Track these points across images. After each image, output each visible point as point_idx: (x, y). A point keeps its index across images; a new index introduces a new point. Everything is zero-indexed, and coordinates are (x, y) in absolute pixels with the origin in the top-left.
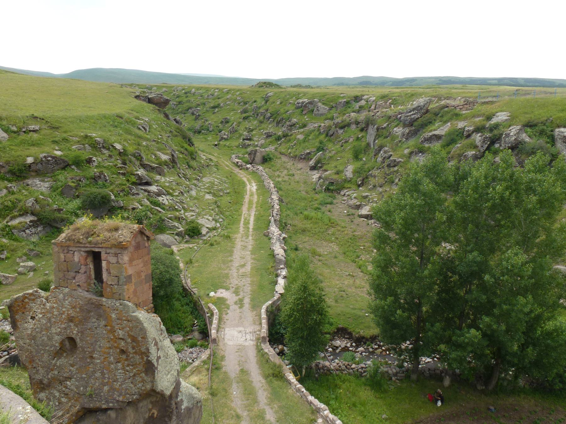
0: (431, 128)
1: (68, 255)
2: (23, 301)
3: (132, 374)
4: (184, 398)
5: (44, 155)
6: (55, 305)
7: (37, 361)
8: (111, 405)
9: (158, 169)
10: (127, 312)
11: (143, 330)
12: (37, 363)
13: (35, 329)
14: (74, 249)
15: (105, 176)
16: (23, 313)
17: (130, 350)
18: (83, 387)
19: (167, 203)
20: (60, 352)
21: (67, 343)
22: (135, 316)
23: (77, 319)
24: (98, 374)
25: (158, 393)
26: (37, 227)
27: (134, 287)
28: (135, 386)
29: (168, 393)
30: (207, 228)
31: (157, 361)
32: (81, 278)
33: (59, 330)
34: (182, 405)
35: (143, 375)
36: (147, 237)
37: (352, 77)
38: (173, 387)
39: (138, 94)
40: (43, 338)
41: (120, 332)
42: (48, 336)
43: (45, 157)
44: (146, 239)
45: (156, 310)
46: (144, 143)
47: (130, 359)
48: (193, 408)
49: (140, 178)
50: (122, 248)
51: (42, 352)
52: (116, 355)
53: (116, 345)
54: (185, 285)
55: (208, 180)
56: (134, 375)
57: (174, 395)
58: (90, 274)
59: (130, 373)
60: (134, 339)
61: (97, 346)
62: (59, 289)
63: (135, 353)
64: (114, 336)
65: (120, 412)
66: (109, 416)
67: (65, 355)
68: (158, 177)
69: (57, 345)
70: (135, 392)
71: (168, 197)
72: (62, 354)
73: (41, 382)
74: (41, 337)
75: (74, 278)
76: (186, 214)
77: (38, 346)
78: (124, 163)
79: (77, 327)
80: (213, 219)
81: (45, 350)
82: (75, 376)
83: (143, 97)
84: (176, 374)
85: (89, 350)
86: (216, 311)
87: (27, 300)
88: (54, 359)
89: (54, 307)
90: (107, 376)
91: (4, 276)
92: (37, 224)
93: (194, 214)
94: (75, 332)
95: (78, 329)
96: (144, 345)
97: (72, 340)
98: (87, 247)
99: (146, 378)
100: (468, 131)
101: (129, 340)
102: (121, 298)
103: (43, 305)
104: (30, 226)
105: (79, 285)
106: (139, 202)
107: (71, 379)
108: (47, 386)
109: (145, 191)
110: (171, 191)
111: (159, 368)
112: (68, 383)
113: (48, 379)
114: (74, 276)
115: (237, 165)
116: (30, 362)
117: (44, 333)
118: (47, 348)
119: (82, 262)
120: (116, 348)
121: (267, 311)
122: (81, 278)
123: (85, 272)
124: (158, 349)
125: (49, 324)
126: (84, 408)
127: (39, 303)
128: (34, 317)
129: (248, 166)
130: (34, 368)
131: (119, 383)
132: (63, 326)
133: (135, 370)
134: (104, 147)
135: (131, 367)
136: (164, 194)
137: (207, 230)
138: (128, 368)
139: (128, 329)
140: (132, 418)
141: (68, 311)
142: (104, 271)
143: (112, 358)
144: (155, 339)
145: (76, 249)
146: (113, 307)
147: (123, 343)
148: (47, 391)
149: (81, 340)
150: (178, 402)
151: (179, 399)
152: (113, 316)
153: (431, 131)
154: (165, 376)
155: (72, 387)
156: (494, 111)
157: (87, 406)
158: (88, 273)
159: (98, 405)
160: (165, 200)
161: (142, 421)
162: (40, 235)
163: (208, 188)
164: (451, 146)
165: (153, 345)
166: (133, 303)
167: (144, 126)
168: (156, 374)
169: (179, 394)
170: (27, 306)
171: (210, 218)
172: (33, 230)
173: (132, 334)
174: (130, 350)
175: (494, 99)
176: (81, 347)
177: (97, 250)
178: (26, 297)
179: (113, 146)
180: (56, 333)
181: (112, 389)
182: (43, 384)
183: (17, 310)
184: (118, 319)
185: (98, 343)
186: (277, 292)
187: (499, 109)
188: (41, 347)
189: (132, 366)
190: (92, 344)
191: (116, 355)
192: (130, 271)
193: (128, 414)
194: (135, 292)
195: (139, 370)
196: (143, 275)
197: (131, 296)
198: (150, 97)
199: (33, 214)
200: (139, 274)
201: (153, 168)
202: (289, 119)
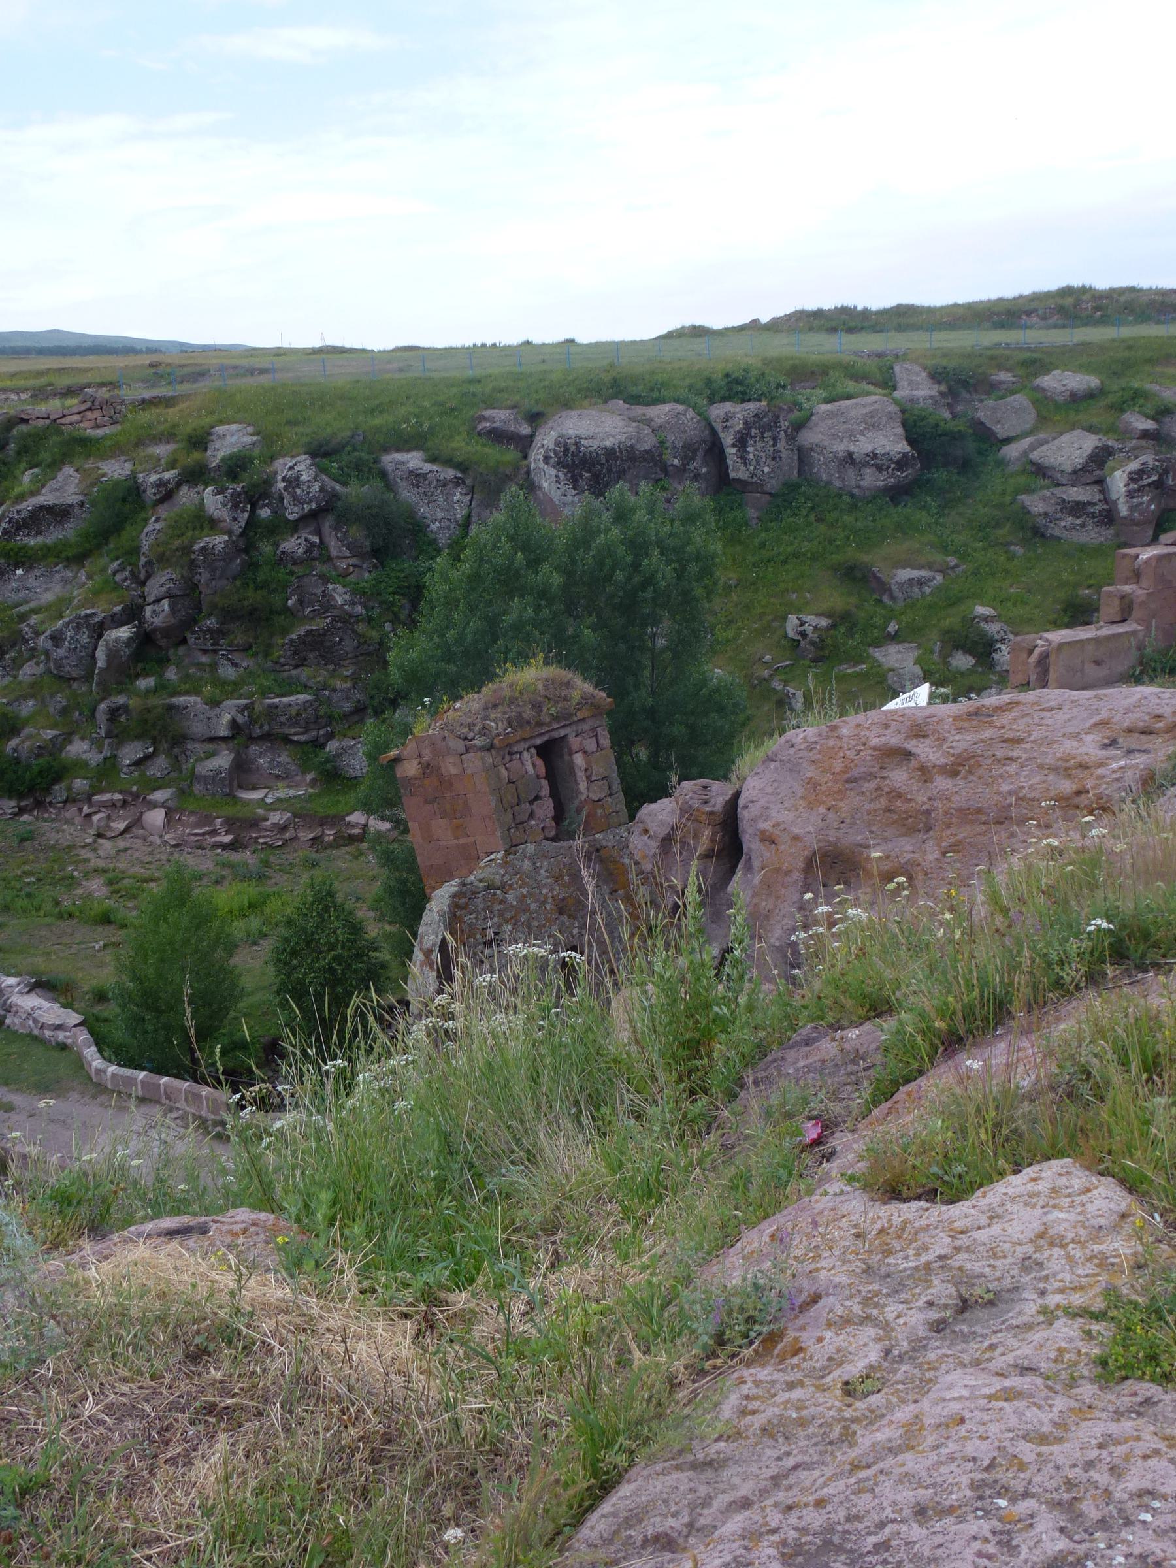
0: (17, 490)
1: (515, 764)
6: (525, 891)
14: (521, 746)
37: (440, 344)
75: (532, 815)
79: (575, 918)
89: (524, 896)
100: (161, 484)
127: (481, 906)
141: (552, 890)
142: (580, 774)
153: (21, 497)
156: (206, 421)
164: (129, 531)
175: (181, 389)
177: (562, 733)
187: (215, 417)
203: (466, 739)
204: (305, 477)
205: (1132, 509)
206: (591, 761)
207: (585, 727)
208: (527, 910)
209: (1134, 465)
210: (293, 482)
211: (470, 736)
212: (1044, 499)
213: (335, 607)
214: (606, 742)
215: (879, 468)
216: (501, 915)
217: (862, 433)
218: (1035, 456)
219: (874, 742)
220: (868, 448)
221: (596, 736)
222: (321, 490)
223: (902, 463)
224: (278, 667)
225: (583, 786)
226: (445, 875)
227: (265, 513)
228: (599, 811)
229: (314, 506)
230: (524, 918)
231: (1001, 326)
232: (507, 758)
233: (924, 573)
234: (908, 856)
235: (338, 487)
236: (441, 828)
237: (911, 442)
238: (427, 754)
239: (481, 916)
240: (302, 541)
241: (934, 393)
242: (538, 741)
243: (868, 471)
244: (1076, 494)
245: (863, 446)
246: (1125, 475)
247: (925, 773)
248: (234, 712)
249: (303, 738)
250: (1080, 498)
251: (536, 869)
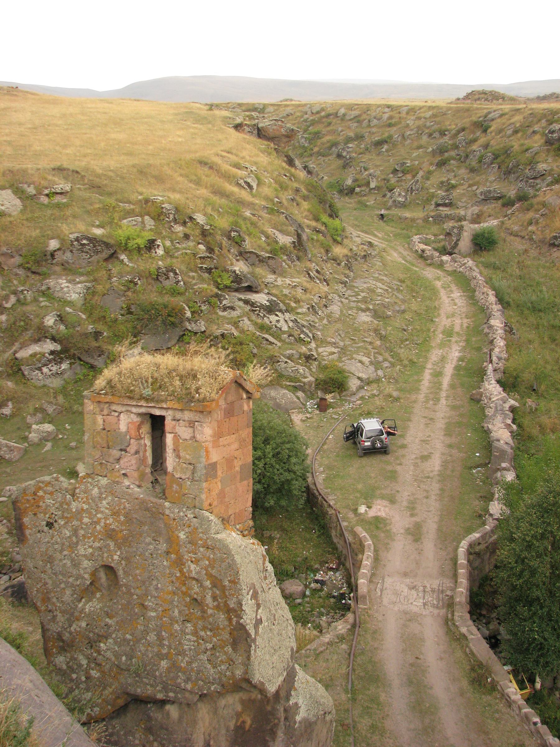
2: (35, 494)
3: (209, 646)
4: (300, 702)
5: (76, 235)
6: (85, 507)
7: (54, 600)
8: (171, 694)
9: (271, 262)
10: (206, 532)
11: (233, 568)
12: (54, 604)
13: (53, 544)
14: (119, 408)
15: (176, 274)
16: (35, 514)
17: (209, 599)
18: (126, 656)
19: (285, 328)
20: (89, 590)
21: (102, 575)
22: (220, 540)
23: (120, 535)
24: (152, 637)
25: (255, 687)
26: (61, 363)
27: (219, 484)
28: (214, 668)
29: (272, 688)
30: (359, 378)
31: (256, 627)
32: (129, 462)
33: (90, 550)
34: (296, 714)
35: (229, 649)
36: (247, 392)
38: (281, 679)
39: (238, 121)
40: (64, 562)
41: (193, 566)
42: (73, 560)
43: (77, 240)
44: (245, 396)
45: (260, 533)
46: (248, 214)
47: (209, 617)
48: (315, 723)
49: (237, 279)
50: (202, 412)
51: (63, 586)
52: (183, 608)
53: (184, 589)
54: (312, 486)
55: (365, 286)
56: (213, 648)
57: (283, 694)
58: (144, 455)
59: (207, 642)
60: (216, 583)
61: (152, 588)
62: (93, 479)
63: (218, 607)
64: (181, 571)
65: (186, 709)
66: (168, 713)
67: (98, 595)
68: (270, 278)
69: (87, 576)
70: (214, 679)
71: (287, 315)
72: (93, 593)
73: (60, 637)
74: (61, 560)
75: (118, 460)
76: (320, 350)
77: (55, 574)
78: (210, 250)
79: (120, 548)
80: (371, 363)
81: (67, 583)
82: (114, 636)
83: (248, 126)
84: (288, 655)
85: (138, 591)
86: (369, 542)
87: (41, 493)
88: (80, 601)
89: (82, 509)
90: (166, 642)
91: (7, 446)
92: (62, 358)
93: (336, 350)
94: (116, 557)
95: (122, 553)
96: (233, 595)
97: (109, 569)
98: (141, 406)
99: (234, 656)
101: (208, 583)
102: (197, 504)
103: (67, 504)
104: (50, 361)
105: (124, 475)
106: (236, 324)
107: (107, 638)
108: (68, 646)
109: (246, 302)
110: (293, 305)
111: (259, 641)
112: (102, 645)
113: (70, 633)
114: (117, 456)
115: (422, 256)
116: (43, 600)
117: (65, 553)
118: (71, 580)
119: (133, 433)
120: (184, 594)
121: (469, 553)
122: (129, 462)
123: (137, 452)
124: (258, 606)
125: (74, 539)
126: (128, 694)
127: (59, 499)
128: (52, 524)
129: (445, 258)
130: (50, 611)
131: (187, 659)
132: (97, 544)
133: (215, 639)
134: (175, 220)
135: (208, 633)
136: (280, 311)
137: (358, 383)
138: (202, 633)
139: (207, 562)
140: (207, 723)
141: (106, 519)
143: (176, 611)
144: (253, 586)
145: (124, 409)
146: (182, 519)
147: (196, 588)
148: (68, 655)
149: (125, 572)
150: (289, 706)
151: (291, 703)
152: (182, 535)
154: (267, 657)
155: (109, 654)
157: (131, 690)
158: (141, 454)
159: (149, 691)
160: (282, 321)
161: (223, 732)
162: (66, 376)
163: (365, 300)
165: (249, 597)
166: (216, 516)
167: (249, 180)
168: (252, 652)
169: (293, 693)
170: (41, 504)
171: (366, 360)
172: (54, 368)
173: (214, 572)
174: (209, 599)
176: (125, 585)
177: (157, 412)
178: (40, 488)
179: (191, 218)
180: (85, 556)
181: (174, 666)
182: (63, 641)
183: (26, 508)
184: (190, 543)
185: (155, 583)
186: (491, 515)
188: (61, 577)
189: (211, 630)
190: (144, 582)
191: (183, 608)
192: (215, 457)
193: (200, 715)
194: (222, 495)
195: (222, 640)
196: (237, 465)
197: (215, 503)
198: (260, 125)
199: (54, 339)
200: (229, 461)
201: (262, 260)
202: (532, 163)
208: (81, 520)
230: (75, 523)
239: (56, 505)
251: (101, 499)
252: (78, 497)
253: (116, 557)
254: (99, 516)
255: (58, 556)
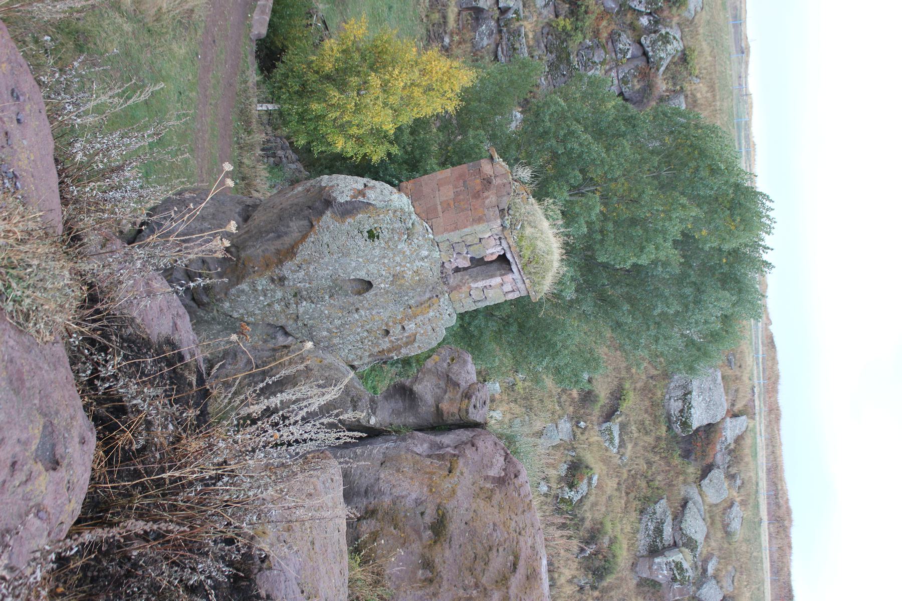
1: (492, 242)
6: (408, 253)
89: (404, 252)
94: (382, 286)
117: (361, 260)
120: (387, 325)
141: (409, 269)
203: (509, 209)
204: (669, 47)
205: (659, 563)
206: (499, 289)
207: (520, 285)
209: (686, 565)
210: (666, 39)
211: (510, 212)
212: (665, 512)
213: (585, 70)
214: (511, 297)
215: (682, 411)
216: (390, 239)
217: (704, 399)
218: (690, 504)
219: (522, 543)
220: (694, 403)
221: (513, 291)
222: (661, 58)
223: (685, 425)
224: (545, 35)
225: (480, 284)
226: (415, 198)
227: (644, 21)
228: (463, 295)
229: (650, 54)
231: (769, 471)
232: (497, 237)
233: (617, 441)
234: (445, 577)
235: (662, 69)
236: (447, 193)
237: (698, 430)
238: (497, 182)
240: (627, 47)
241: (729, 441)
242: (509, 256)
243: (680, 404)
244: (668, 530)
245: (696, 399)
246: (679, 560)
247: (503, 581)
248: (515, 7)
249: (500, 53)
250: (665, 533)
251: (423, 259)
252: (411, 244)
253: (382, 286)
254: (408, 265)
255: (354, 257)
